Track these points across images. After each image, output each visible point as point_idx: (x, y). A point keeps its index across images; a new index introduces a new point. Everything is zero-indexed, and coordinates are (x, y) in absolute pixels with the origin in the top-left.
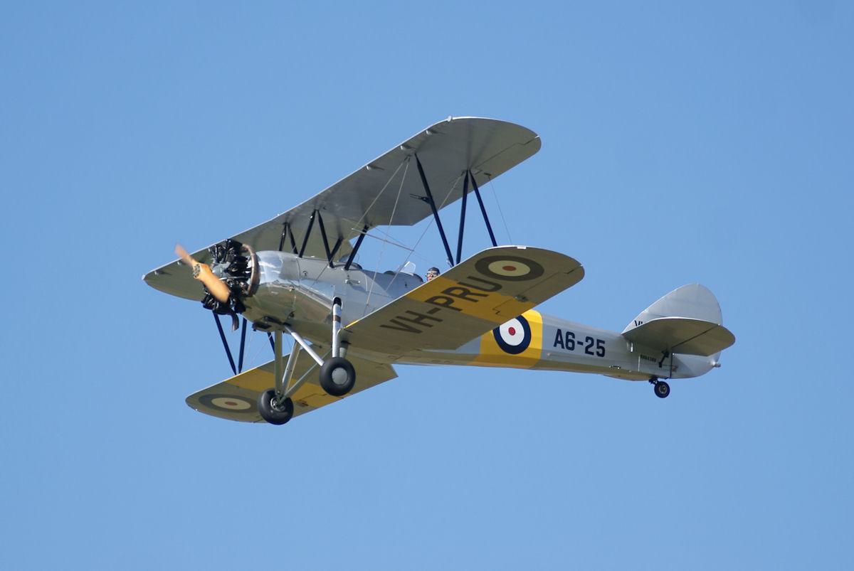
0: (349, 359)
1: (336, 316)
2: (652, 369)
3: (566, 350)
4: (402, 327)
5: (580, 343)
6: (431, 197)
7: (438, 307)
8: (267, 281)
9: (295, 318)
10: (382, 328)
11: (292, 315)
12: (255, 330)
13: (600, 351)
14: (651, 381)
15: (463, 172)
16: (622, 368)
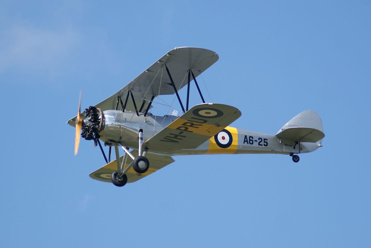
0: (147, 157)
1: (140, 137)
3: (249, 145)
4: (169, 140)
5: (256, 141)
6: (173, 83)
7: (183, 131)
8: (108, 124)
9: (122, 139)
10: (161, 141)
11: (121, 138)
12: (105, 146)
13: (266, 144)
14: (291, 155)
15: (188, 71)
16: (276, 151)
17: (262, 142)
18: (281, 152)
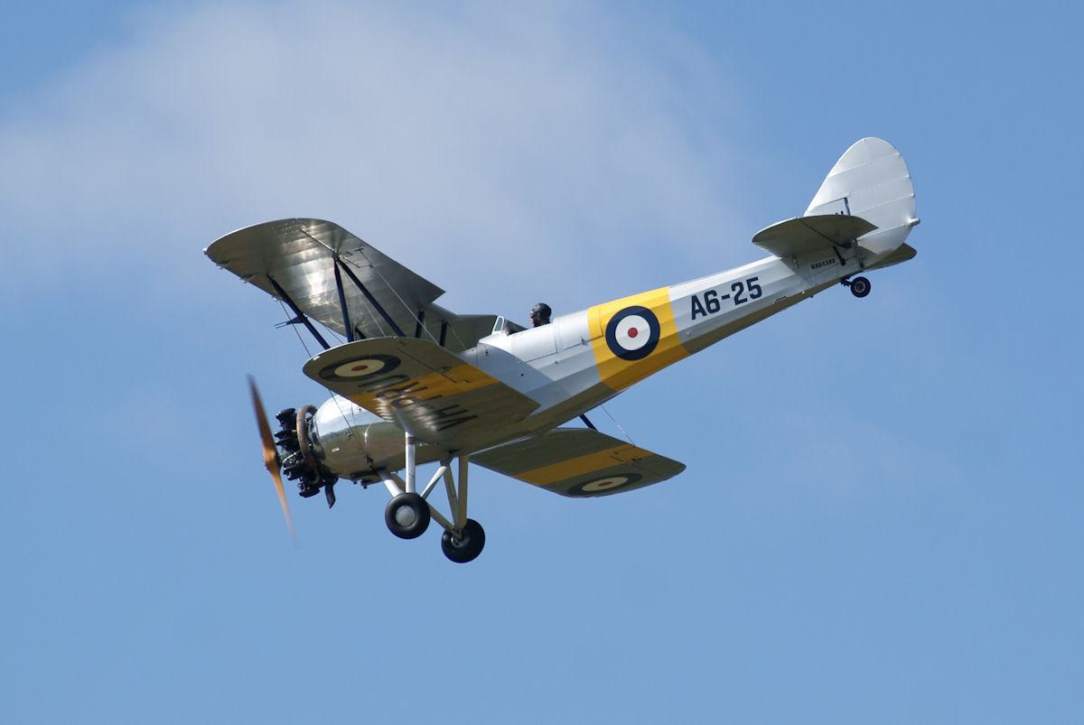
1: (409, 438)
3: (710, 316)
9: (375, 461)
11: (370, 460)
12: (365, 488)
13: (755, 292)
14: (848, 284)
18: (806, 292)
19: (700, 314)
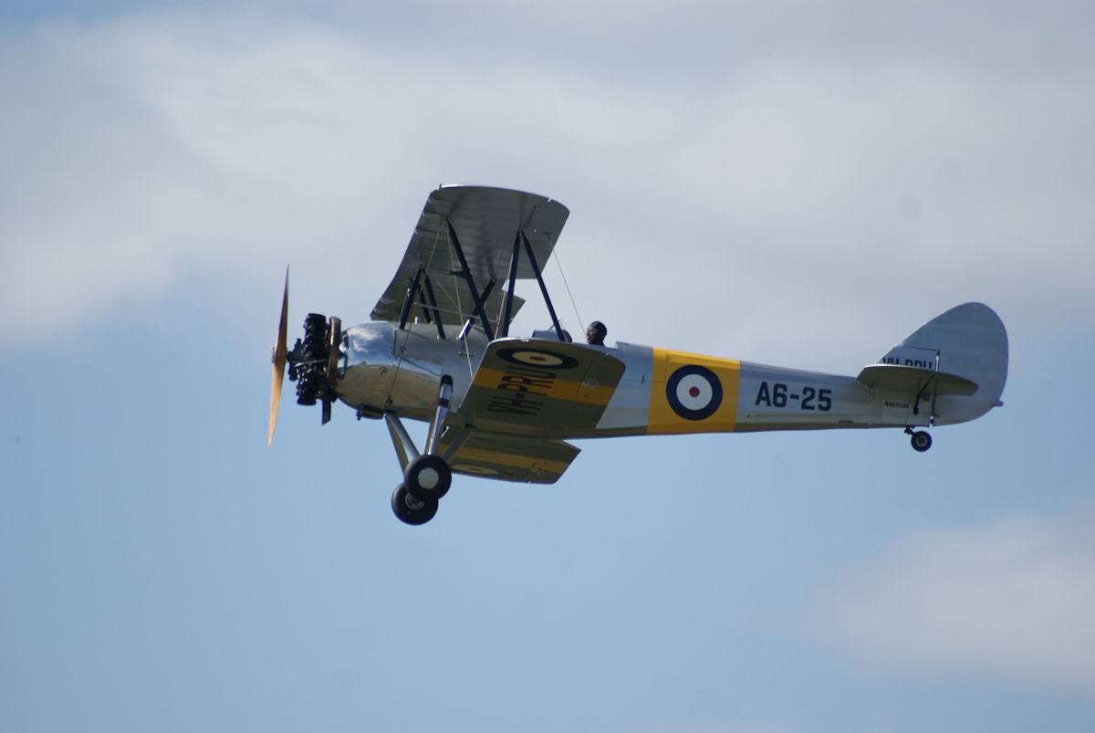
2: (906, 415)
3: (773, 409)
5: (795, 397)
9: (394, 404)
11: (390, 401)
12: (359, 419)
13: (824, 404)
14: (908, 431)
17: (813, 400)
19: (765, 402)
